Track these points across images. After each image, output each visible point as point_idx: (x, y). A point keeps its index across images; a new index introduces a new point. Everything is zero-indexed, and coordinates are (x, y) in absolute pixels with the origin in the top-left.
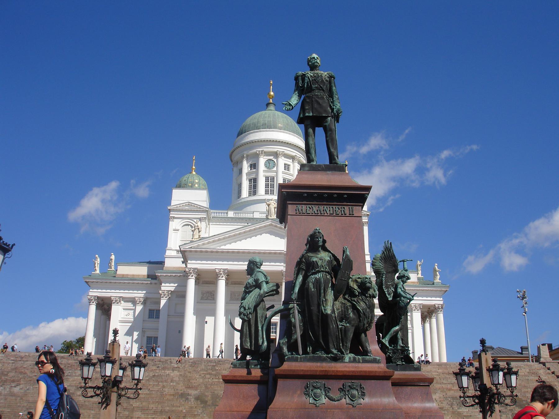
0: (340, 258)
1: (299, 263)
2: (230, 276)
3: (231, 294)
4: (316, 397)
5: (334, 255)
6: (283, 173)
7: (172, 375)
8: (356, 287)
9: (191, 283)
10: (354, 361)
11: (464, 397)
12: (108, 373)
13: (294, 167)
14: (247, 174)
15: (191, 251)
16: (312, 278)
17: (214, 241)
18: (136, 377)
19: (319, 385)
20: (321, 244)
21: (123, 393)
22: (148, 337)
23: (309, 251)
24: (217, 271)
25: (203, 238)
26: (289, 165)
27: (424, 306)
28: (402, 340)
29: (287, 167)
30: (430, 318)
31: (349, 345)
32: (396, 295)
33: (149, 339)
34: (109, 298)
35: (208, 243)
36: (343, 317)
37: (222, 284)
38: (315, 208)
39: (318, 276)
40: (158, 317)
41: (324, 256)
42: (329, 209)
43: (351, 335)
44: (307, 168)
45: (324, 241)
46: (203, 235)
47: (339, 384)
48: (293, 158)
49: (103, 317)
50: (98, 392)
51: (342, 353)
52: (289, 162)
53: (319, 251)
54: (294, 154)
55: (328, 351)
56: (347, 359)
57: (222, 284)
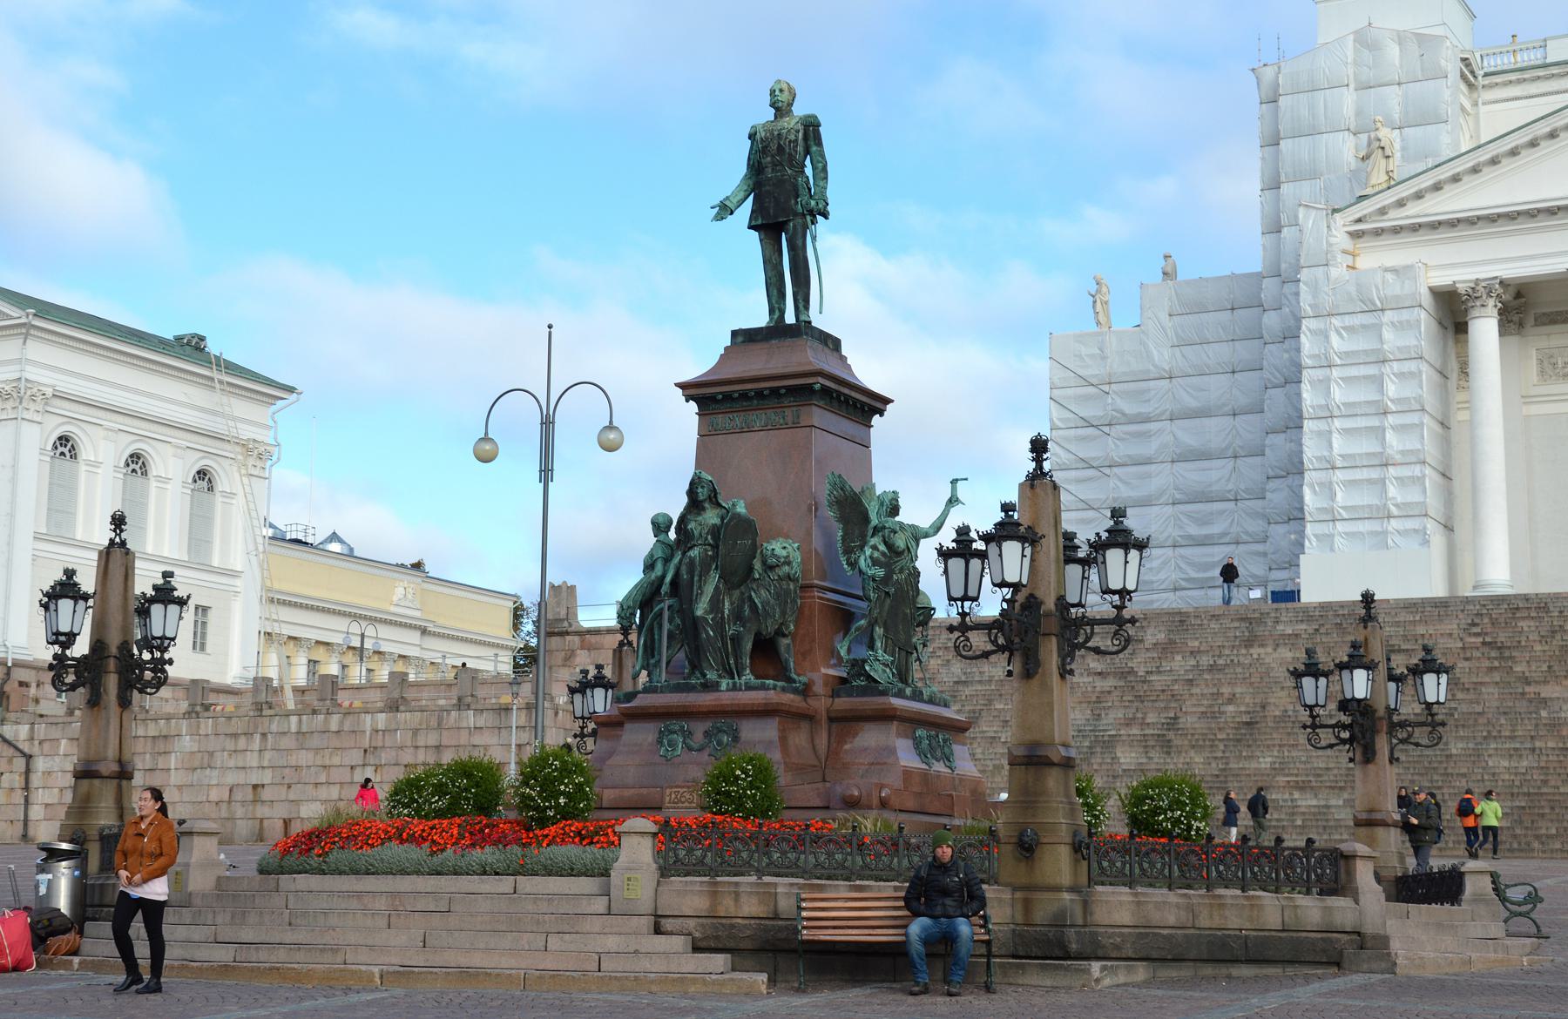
4: (672, 744)
10: (734, 688)
11: (1314, 726)
17: (1437, 187)
19: (677, 728)
35: (1419, 196)
36: (737, 616)
38: (739, 420)
41: (711, 517)
42: (758, 418)
43: (748, 646)
44: (740, 339)
47: (708, 725)
53: (704, 509)
55: (704, 675)
56: (724, 686)
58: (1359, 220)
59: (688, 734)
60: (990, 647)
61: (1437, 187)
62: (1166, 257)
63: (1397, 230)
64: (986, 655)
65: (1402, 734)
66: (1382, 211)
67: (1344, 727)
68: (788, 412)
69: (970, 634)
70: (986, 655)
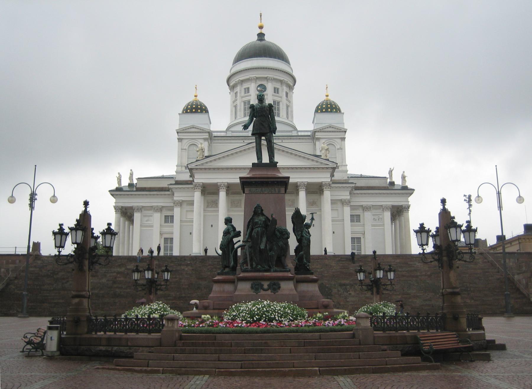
0: (270, 218)
1: (249, 222)
2: (229, 188)
3: (231, 203)
5: (267, 217)
6: (273, 95)
7: (186, 269)
8: (278, 234)
9: (197, 195)
10: (276, 271)
12: (150, 277)
13: (283, 89)
14: (242, 97)
15: (197, 169)
16: (256, 230)
17: (215, 160)
18: (166, 278)
20: (260, 212)
21: (159, 287)
22: (165, 238)
24: (219, 184)
25: (207, 157)
26: (278, 89)
27: (393, 207)
28: (306, 258)
29: (276, 90)
30: (399, 216)
31: (274, 263)
32: (302, 236)
33: (166, 239)
34: (131, 208)
35: (211, 161)
37: (222, 195)
38: (259, 189)
39: (259, 229)
40: (172, 221)
41: (262, 218)
45: (262, 210)
46: (206, 154)
48: (281, 82)
49: (127, 223)
50: (144, 288)
51: (270, 267)
52: (278, 85)
54: (282, 79)
57: (222, 195)
58: (197, 166)
59: (262, 286)
61: (215, 160)
62: (131, 170)
63: (205, 169)
64: (431, 262)
65: (384, 287)
66: (202, 164)
67: (370, 285)
68: (277, 189)
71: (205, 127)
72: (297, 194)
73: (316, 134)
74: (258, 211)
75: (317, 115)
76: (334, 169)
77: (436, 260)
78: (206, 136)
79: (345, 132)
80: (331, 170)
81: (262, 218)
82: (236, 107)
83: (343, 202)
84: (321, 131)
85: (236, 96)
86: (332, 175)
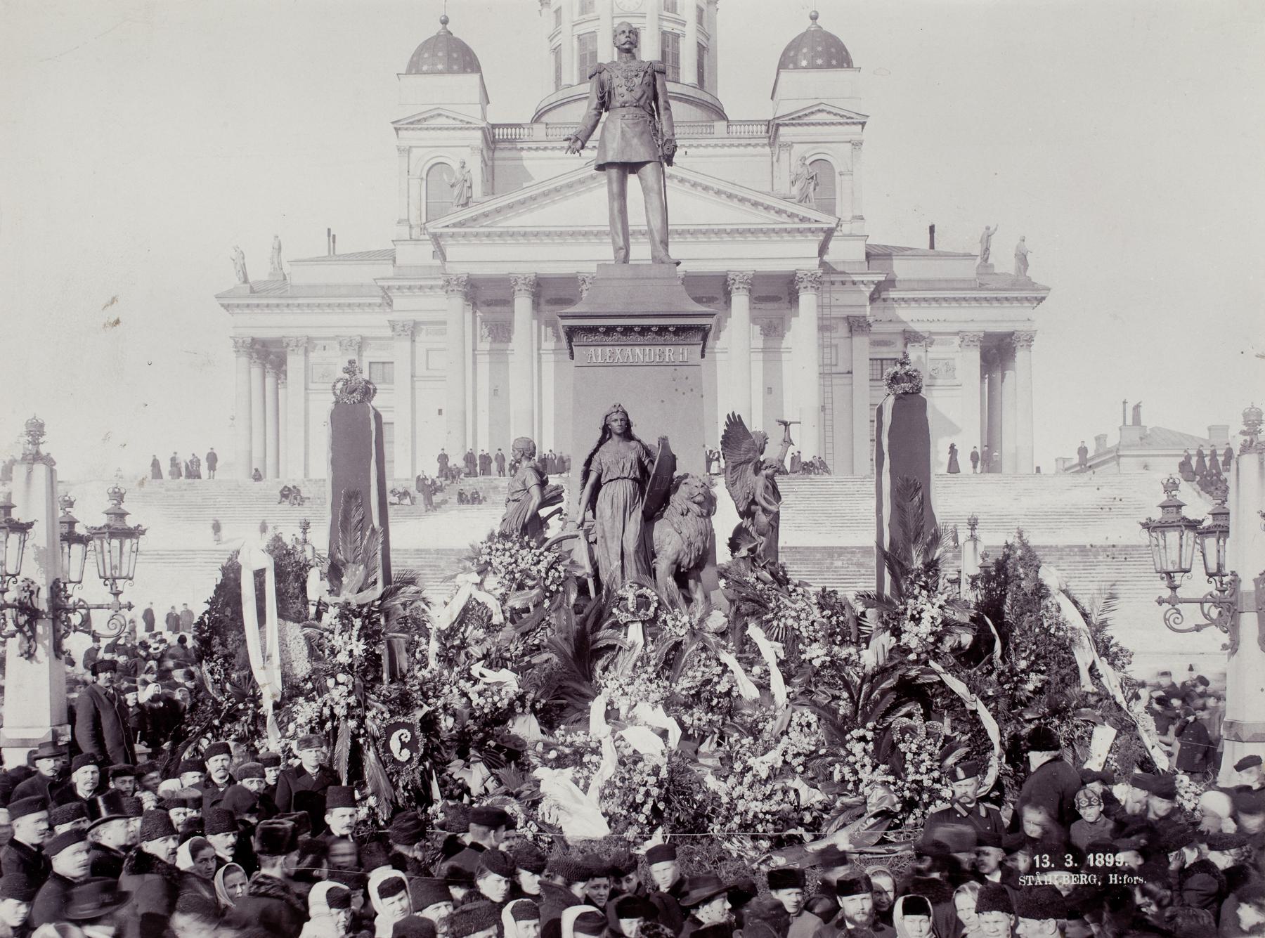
23: (602, 442)
45: (627, 426)
57: (523, 304)
60: (1202, 621)
64: (1198, 628)
69: (1179, 606)
70: (1198, 628)
71: (474, 113)
72: (728, 302)
73: (782, 130)
74: (618, 429)
75: (783, 74)
76: (829, 233)
77: (1213, 622)
78: (477, 138)
79: (863, 124)
80: (822, 237)
81: (630, 453)
82: (557, 51)
83: (856, 325)
84: (797, 119)
85: (558, 22)
86: (823, 250)
